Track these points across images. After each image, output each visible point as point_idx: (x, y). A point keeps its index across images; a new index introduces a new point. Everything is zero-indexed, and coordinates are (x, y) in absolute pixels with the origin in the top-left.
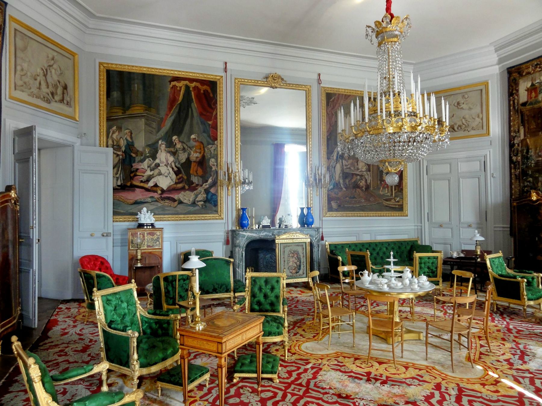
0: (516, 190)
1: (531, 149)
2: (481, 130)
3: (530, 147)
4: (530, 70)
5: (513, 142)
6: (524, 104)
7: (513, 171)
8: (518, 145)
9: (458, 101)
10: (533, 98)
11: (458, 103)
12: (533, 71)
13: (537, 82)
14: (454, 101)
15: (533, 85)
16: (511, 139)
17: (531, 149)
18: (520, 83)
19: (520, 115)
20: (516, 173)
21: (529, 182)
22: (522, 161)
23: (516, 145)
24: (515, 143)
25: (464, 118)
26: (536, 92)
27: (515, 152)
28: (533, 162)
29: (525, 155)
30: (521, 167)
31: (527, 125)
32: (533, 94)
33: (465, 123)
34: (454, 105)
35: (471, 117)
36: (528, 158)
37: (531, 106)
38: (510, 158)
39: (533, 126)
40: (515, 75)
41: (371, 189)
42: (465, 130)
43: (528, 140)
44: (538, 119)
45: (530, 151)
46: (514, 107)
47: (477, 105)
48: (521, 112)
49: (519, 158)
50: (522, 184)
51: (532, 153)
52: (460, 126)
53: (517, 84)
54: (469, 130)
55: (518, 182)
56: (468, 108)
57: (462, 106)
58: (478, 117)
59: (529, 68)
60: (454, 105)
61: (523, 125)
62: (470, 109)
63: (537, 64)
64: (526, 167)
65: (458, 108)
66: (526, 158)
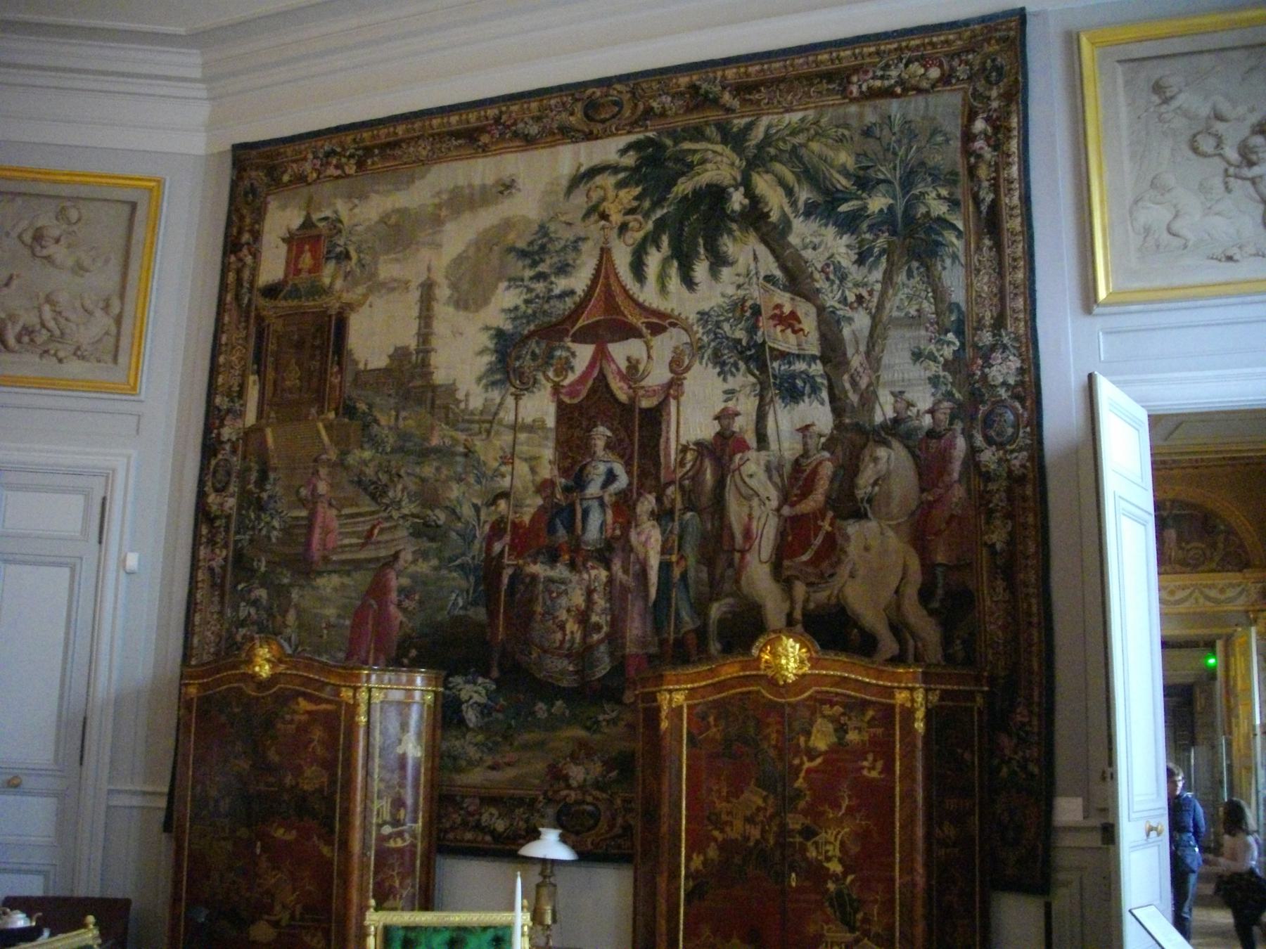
0: (207, 635)
1: (275, 469)
2: (111, 365)
3: (274, 461)
4: (307, 167)
5: (219, 434)
6: (272, 291)
7: (203, 552)
8: (234, 451)
9: (39, 224)
10: (304, 275)
11: (38, 237)
12: (315, 175)
13: (323, 215)
14: (24, 224)
15: (308, 224)
16: (213, 418)
17: (275, 469)
18: (270, 207)
19: (253, 329)
20: (214, 564)
21: (255, 603)
22: (239, 514)
24: (225, 437)
25: (48, 300)
26: (314, 257)
27: (219, 477)
28: (276, 523)
29: (250, 493)
30: (233, 537)
31: (271, 375)
32: (307, 260)
33: (51, 324)
34: (20, 237)
35: (77, 304)
36: (261, 507)
37: (295, 303)
38: (201, 495)
39: (292, 378)
40: (257, 176)
42: (46, 352)
43: (269, 432)
44: (312, 357)
45: (272, 476)
46: (237, 297)
47: (107, 261)
48: (260, 319)
49: (231, 502)
50: (229, 612)
51: (275, 486)
52: (28, 331)
53: (260, 214)
54: (61, 354)
55: (216, 599)
56: (70, 262)
57: (52, 249)
58: (106, 308)
59: (305, 159)
60: (20, 237)
61: (258, 372)
62: (79, 268)
63: (332, 153)
64: (251, 541)
65: (34, 255)
66: (253, 503)
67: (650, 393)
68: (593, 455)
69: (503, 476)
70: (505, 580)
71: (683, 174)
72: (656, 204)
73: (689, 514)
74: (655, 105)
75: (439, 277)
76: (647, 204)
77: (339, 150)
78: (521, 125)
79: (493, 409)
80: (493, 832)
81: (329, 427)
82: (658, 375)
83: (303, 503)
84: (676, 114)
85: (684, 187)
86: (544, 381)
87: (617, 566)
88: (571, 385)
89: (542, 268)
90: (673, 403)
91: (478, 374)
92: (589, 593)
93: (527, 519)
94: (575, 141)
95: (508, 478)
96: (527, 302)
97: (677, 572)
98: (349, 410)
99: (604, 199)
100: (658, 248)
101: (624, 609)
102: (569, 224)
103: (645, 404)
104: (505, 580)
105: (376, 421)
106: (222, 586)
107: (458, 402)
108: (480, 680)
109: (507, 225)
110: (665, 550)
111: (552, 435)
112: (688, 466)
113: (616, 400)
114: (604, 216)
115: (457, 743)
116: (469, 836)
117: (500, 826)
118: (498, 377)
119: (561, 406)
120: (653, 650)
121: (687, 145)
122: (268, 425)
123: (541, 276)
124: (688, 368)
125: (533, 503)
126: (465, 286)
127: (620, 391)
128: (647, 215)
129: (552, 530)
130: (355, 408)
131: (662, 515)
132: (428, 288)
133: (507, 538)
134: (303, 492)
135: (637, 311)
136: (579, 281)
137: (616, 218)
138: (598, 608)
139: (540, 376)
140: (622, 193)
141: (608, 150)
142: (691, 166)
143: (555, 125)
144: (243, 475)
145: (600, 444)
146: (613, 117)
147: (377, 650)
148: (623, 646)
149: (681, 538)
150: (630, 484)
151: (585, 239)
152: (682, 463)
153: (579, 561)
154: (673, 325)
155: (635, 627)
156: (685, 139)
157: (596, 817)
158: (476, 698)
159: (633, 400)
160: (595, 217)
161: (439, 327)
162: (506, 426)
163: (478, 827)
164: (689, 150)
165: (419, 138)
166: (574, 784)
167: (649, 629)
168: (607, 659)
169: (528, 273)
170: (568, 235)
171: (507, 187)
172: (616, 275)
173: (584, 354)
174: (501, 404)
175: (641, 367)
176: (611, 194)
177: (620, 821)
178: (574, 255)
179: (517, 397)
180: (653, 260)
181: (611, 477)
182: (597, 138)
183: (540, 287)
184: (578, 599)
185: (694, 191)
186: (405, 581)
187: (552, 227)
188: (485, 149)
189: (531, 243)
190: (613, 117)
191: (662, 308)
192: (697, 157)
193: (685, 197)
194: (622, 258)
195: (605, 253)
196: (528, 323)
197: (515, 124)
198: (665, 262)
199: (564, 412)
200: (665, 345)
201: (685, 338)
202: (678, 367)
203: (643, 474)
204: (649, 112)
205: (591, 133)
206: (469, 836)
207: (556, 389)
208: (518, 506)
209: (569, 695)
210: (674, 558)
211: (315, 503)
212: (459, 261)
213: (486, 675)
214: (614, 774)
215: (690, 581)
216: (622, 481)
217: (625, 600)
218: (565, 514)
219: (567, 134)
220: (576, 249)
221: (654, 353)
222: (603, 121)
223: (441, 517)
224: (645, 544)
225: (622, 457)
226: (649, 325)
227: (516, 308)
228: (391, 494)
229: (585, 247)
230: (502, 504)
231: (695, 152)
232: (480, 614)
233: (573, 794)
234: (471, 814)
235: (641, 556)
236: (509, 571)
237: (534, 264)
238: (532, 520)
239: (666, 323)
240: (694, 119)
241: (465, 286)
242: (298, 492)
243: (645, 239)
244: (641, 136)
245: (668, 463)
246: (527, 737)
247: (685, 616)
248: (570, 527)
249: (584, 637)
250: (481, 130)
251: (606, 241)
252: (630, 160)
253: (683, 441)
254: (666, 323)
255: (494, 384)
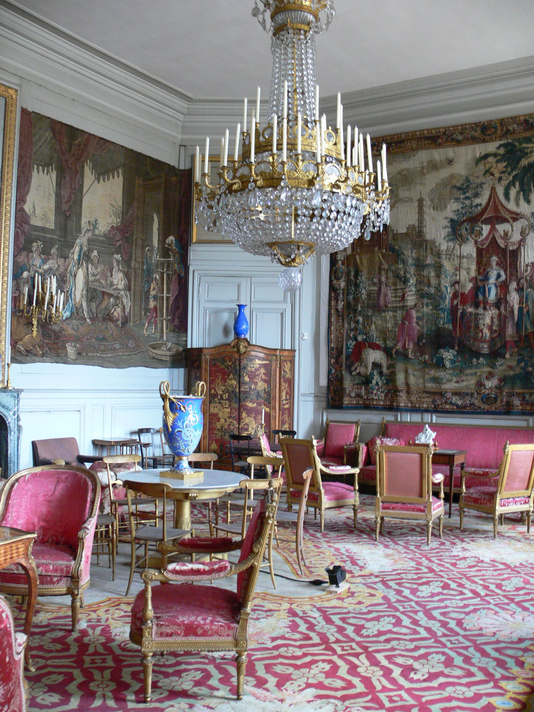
23: (340, 262)
41: (131, 324)
49: (343, 284)
67: (514, 244)
68: (492, 268)
69: (456, 275)
70: (459, 314)
71: (523, 157)
72: (512, 170)
73: (529, 290)
74: (511, 128)
75: (425, 197)
76: (509, 169)
77: (377, 144)
78: (454, 136)
79: (451, 250)
80: (457, 405)
81: (383, 256)
82: (516, 237)
83: (374, 284)
84: (520, 132)
85: (524, 162)
86: (471, 239)
87: (502, 309)
88: (482, 240)
89: (467, 195)
90: (522, 248)
91: (443, 236)
92: (492, 318)
93: (467, 292)
94: (478, 142)
95: (458, 276)
96: (462, 208)
97: (525, 311)
98: (393, 250)
99: (492, 167)
100: (515, 187)
101: (505, 324)
102: (478, 177)
103: (511, 248)
104: (459, 314)
105: (403, 254)
106: (343, 316)
107: (436, 247)
108: (451, 351)
109: (452, 176)
110: (521, 302)
111: (475, 260)
112: (529, 272)
113: (499, 246)
114: (492, 174)
115: (442, 374)
116: (447, 407)
117: (460, 403)
118: (452, 237)
119: (478, 249)
120: (516, 339)
121: (524, 145)
122: (357, 254)
123: (467, 198)
124: (528, 235)
125: (469, 286)
126: (436, 201)
127: (502, 243)
128: (509, 174)
129: (477, 296)
130: (394, 249)
131: (520, 290)
132: (421, 202)
133: (459, 299)
134: (375, 280)
135: (507, 213)
136: (483, 200)
137: (497, 175)
138: (495, 324)
139: (469, 237)
140: (499, 165)
141: (491, 147)
142: (527, 154)
143: (469, 136)
144: (348, 274)
145: (494, 264)
146: (494, 133)
147: (409, 340)
148: (505, 338)
149: (527, 298)
150: (506, 278)
151: (484, 183)
152: (526, 271)
153: (488, 307)
154: (522, 218)
155: (510, 330)
156: (523, 143)
157: (496, 399)
158: (449, 357)
159: (506, 246)
160: (488, 175)
161: (427, 219)
162: (457, 256)
163: (451, 403)
164: (525, 148)
165: (411, 139)
166: (487, 387)
167: (515, 332)
168: (499, 343)
169: (462, 196)
170: (478, 181)
171: (450, 162)
172: (498, 198)
173: (486, 229)
174: (454, 248)
175: (509, 234)
176: (494, 165)
177: (505, 400)
178: (480, 189)
179: (460, 246)
180: (513, 192)
181: (499, 276)
182: (487, 142)
183: (467, 202)
184: (488, 321)
185: (529, 164)
186: (420, 315)
187: (471, 178)
188: (440, 144)
189: (463, 185)
190: (494, 133)
191: (517, 211)
192: (529, 150)
193: (525, 167)
194: (500, 191)
195: (493, 189)
196: (463, 216)
197: (452, 135)
198: (518, 193)
199: (480, 252)
200: (518, 225)
201: (526, 223)
202: (523, 234)
203: (511, 274)
204: (508, 131)
205: (484, 139)
206: (447, 407)
207: (476, 242)
208: (463, 286)
209: (483, 355)
210: (524, 306)
211: (380, 285)
212: (432, 191)
213: (453, 348)
214: (502, 384)
215: (531, 316)
216: (503, 277)
217: (505, 320)
218: (481, 290)
219: (474, 140)
220: (481, 187)
221: (514, 229)
222: (489, 135)
223: (432, 291)
224: (512, 301)
225: (502, 268)
226: (512, 218)
227: (458, 210)
228: (411, 281)
229: (485, 186)
230: (457, 286)
231: (528, 148)
232: (450, 326)
233: (487, 391)
234: (449, 399)
235: (511, 305)
236: (461, 311)
237: (464, 193)
238: (469, 291)
239: (518, 217)
240: (528, 134)
241: (436, 201)
242: (372, 280)
243: (509, 183)
244: (505, 142)
245: (521, 271)
246: (469, 371)
247: (528, 326)
248: (484, 295)
249: (491, 335)
250: (438, 137)
251: (494, 184)
252: (502, 151)
253: (526, 262)
254: (518, 217)
255: (451, 240)
